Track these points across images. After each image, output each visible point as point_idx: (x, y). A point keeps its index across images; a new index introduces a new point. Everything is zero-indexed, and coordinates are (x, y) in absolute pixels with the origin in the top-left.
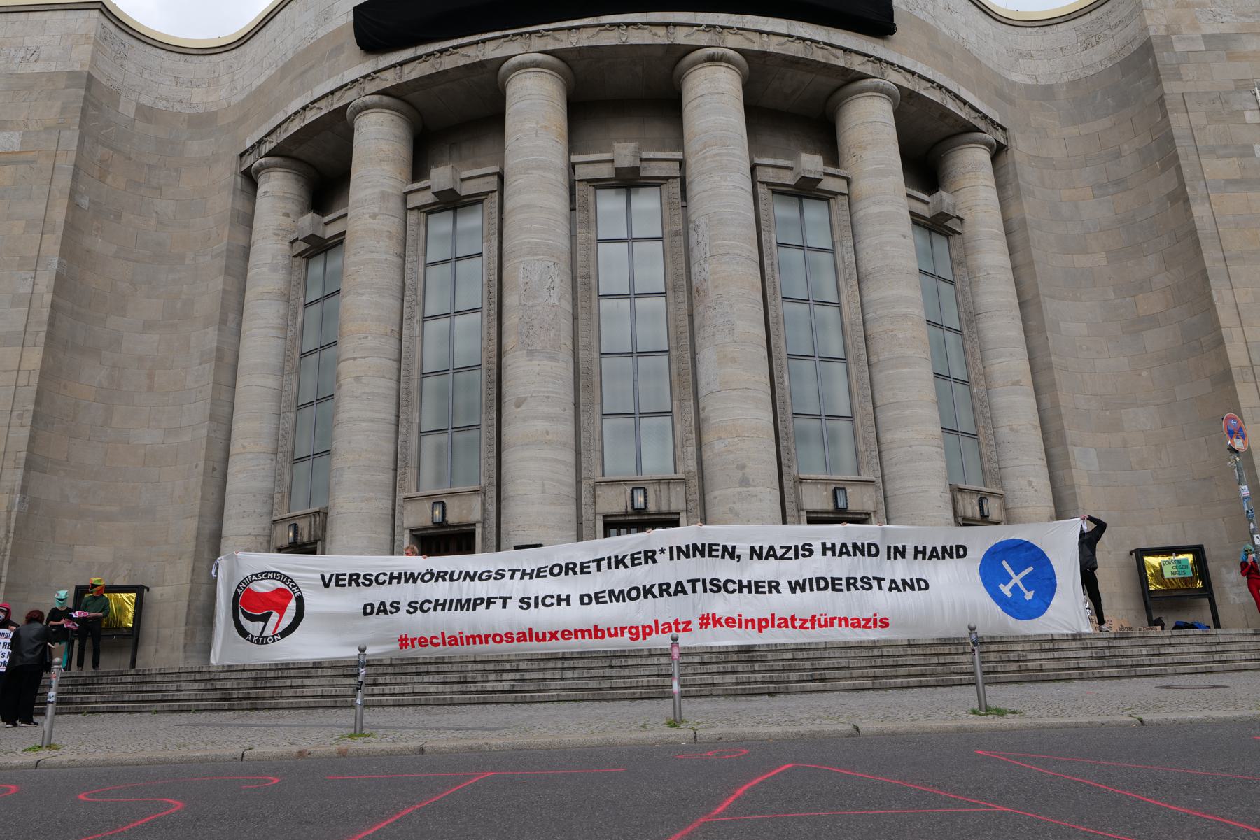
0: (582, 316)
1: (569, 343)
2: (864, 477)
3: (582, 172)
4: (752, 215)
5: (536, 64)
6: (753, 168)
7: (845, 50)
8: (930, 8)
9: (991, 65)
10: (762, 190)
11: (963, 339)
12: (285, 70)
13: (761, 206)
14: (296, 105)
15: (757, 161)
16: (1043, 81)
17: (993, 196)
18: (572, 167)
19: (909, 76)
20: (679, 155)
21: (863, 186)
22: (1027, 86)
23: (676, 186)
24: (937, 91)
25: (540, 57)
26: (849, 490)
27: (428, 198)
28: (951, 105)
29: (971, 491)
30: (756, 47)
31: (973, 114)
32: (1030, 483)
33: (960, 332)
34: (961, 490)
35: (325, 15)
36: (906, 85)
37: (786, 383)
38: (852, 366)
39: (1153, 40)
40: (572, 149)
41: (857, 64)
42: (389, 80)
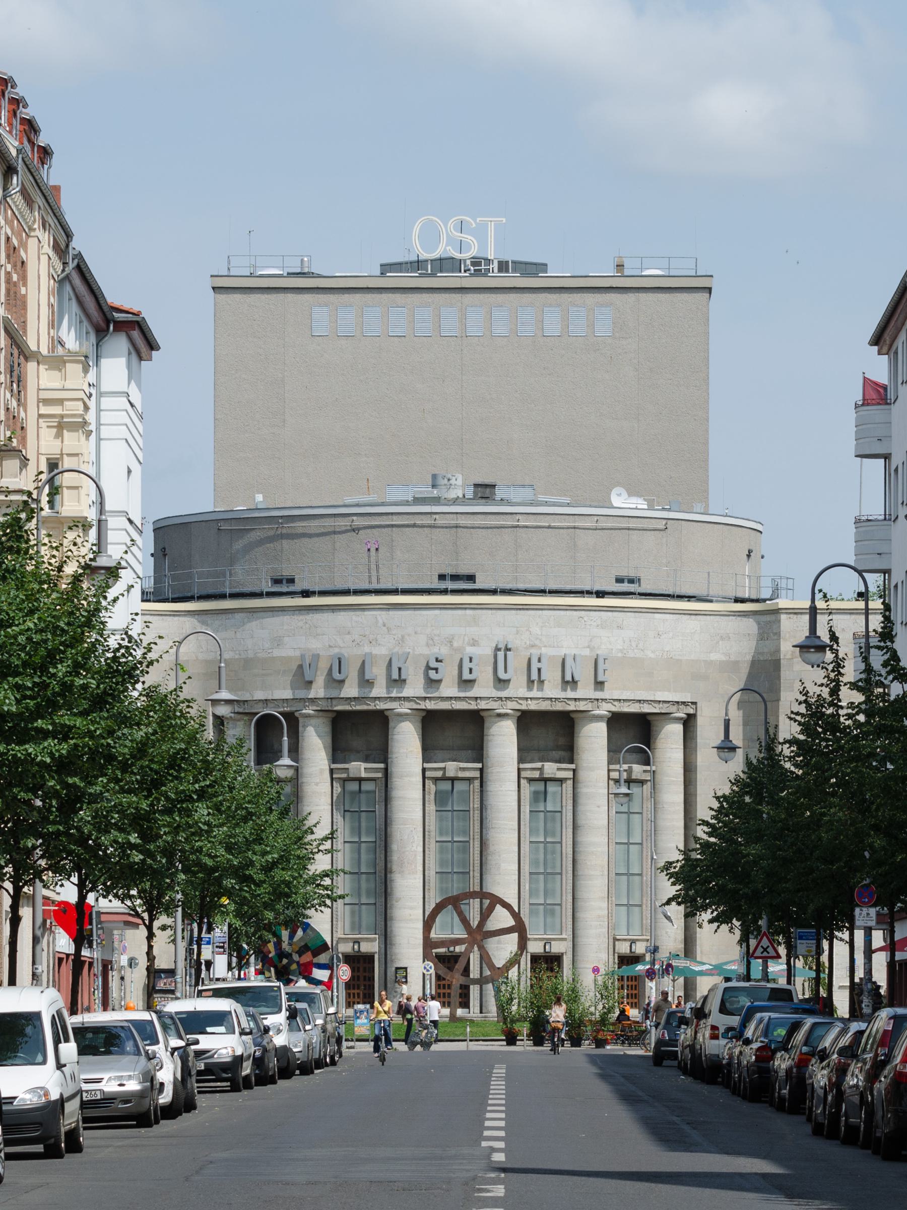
0: (427, 852)
1: (421, 868)
2: (564, 936)
3: (428, 774)
4: (516, 804)
5: (407, 714)
6: (519, 769)
7: (575, 699)
8: (641, 646)
9: (692, 657)
10: (523, 781)
11: (642, 848)
12: (248, 663)
13: (522, 791)
14: (260, 695)
15: (522, 766)
16: (733, 658)
17: (679, 755)
18: (424, 770)
19: (616, 703)
20: (480, 765)
21: (582, 775)
22: (721, 662)
23: (477, 783)
24: (637, 705)
25: (409, 711)
26: (553, 943)
27: (344, 776)
28: (647, 709)
29: (625, 940)
30: (524, 707)
31: (666, 705)
32: (667, 933)
33: (641, 844)
34: (619, 940)
35: (278, 642)
36: (614, 709)
37: (527, 888)
38: (564, 876)
39: (782, 661)
40: (425, 760)
41: (582, 706)
42: (324, 705)
